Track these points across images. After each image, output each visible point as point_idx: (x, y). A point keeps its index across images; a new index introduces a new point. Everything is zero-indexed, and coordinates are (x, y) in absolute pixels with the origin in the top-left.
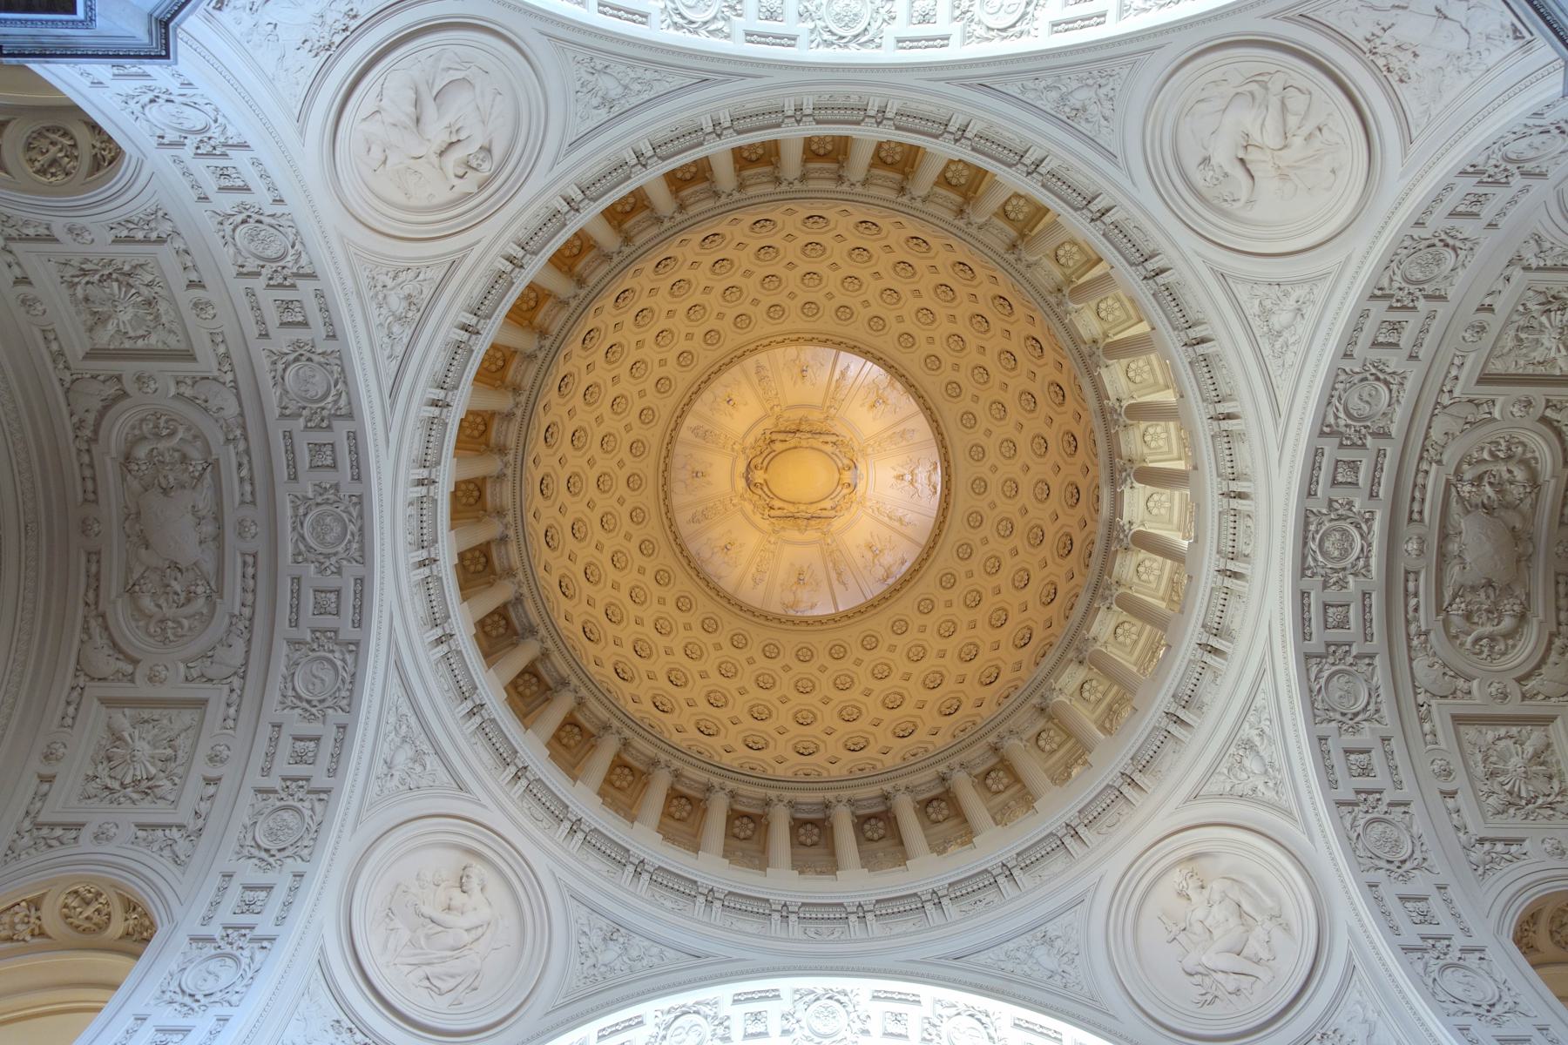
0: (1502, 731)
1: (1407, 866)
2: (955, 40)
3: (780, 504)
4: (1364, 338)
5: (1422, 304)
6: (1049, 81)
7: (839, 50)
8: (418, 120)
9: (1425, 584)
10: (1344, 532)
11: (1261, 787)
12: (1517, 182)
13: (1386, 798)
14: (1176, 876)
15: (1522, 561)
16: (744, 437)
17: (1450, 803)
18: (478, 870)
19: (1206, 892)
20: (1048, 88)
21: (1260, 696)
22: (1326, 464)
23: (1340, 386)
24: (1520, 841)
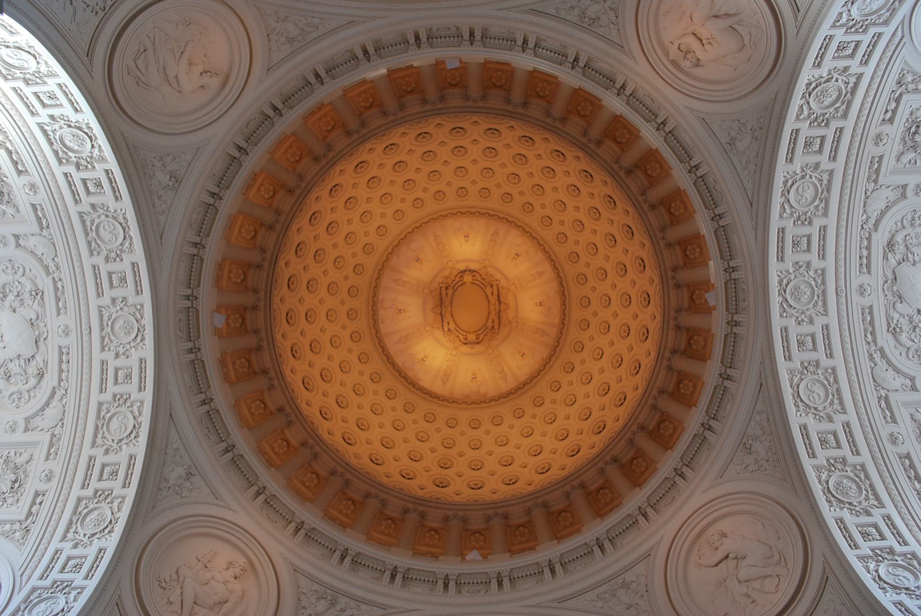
2: (789, 365)
3: (450, 295)
7: (777, 289)
8: (716, 16)
14: (242, 561)
16: (492, 267)
18: (214, 82)
19: (233, 580)
21: (369, 608)
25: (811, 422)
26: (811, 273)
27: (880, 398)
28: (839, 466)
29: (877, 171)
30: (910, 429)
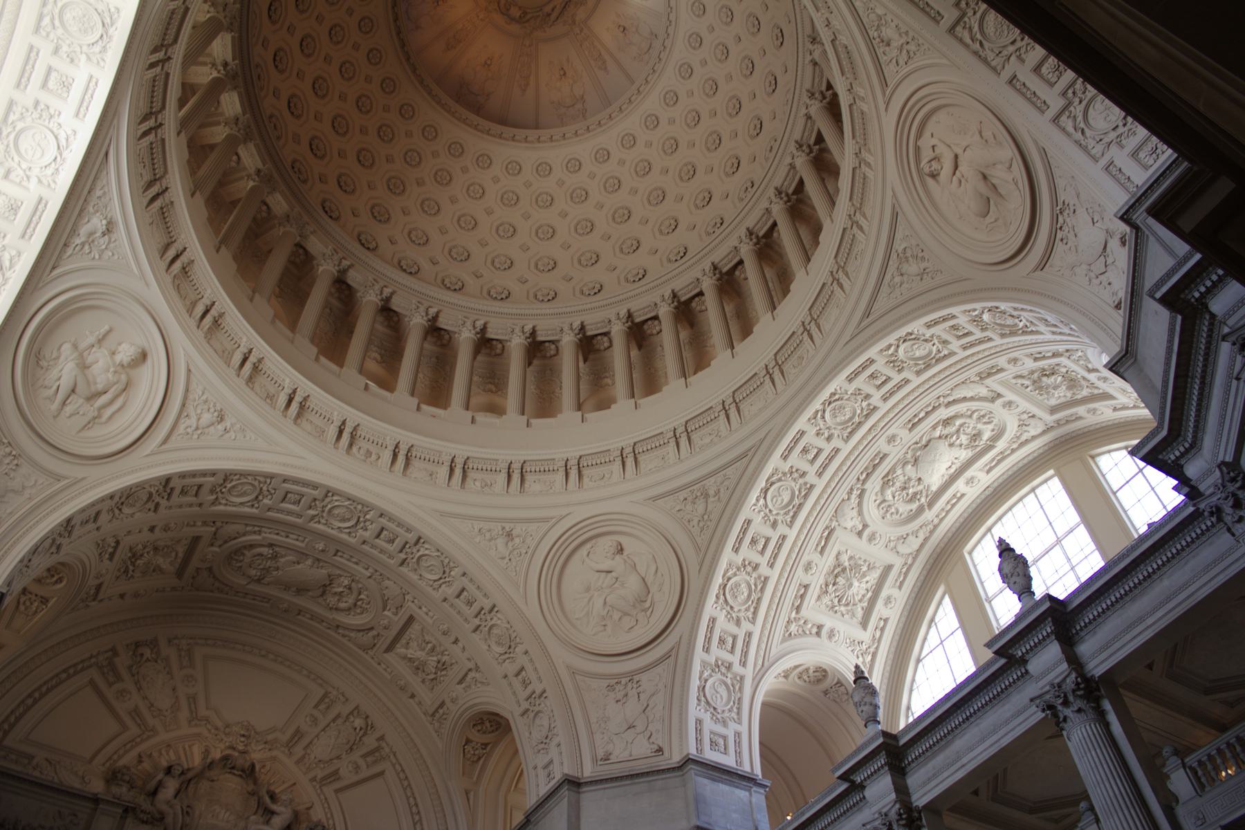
0: (181, 555)
1: (117, 512)
6: (721, 495)
8: (985, 177)
10: (349, 520)
12: (525, 705)
13: (164, 503)
17: (146, 529)
20: (717, 493)
23: (446, 561)
24: (111, 559)
25: (758, 520)
26: (864, 404)
27: (827, 528)
28: (749, 569)
29: (989, 375)
30: (829, 563)
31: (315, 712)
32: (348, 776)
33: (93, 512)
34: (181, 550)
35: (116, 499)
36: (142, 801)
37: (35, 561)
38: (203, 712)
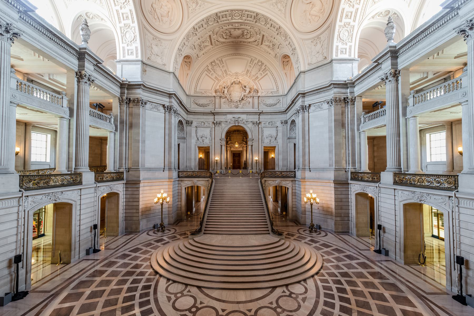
4: (273, 23)
5: (277, 32)
9: (230, 27)
11: (191, 9)
12: (292, 52)
13: (197, 32)
15: (235, 38)
22: (252, 14)
31: (251, 65)
32: (260, 77)
33: (183, 43)
34: (209, 40)
35: (186, 38)
36: (222, 95)
37: (178, 60)
38: (228, 73)
